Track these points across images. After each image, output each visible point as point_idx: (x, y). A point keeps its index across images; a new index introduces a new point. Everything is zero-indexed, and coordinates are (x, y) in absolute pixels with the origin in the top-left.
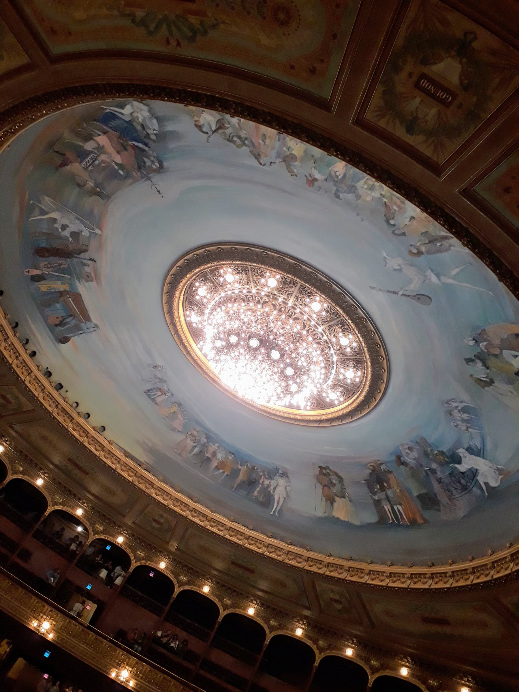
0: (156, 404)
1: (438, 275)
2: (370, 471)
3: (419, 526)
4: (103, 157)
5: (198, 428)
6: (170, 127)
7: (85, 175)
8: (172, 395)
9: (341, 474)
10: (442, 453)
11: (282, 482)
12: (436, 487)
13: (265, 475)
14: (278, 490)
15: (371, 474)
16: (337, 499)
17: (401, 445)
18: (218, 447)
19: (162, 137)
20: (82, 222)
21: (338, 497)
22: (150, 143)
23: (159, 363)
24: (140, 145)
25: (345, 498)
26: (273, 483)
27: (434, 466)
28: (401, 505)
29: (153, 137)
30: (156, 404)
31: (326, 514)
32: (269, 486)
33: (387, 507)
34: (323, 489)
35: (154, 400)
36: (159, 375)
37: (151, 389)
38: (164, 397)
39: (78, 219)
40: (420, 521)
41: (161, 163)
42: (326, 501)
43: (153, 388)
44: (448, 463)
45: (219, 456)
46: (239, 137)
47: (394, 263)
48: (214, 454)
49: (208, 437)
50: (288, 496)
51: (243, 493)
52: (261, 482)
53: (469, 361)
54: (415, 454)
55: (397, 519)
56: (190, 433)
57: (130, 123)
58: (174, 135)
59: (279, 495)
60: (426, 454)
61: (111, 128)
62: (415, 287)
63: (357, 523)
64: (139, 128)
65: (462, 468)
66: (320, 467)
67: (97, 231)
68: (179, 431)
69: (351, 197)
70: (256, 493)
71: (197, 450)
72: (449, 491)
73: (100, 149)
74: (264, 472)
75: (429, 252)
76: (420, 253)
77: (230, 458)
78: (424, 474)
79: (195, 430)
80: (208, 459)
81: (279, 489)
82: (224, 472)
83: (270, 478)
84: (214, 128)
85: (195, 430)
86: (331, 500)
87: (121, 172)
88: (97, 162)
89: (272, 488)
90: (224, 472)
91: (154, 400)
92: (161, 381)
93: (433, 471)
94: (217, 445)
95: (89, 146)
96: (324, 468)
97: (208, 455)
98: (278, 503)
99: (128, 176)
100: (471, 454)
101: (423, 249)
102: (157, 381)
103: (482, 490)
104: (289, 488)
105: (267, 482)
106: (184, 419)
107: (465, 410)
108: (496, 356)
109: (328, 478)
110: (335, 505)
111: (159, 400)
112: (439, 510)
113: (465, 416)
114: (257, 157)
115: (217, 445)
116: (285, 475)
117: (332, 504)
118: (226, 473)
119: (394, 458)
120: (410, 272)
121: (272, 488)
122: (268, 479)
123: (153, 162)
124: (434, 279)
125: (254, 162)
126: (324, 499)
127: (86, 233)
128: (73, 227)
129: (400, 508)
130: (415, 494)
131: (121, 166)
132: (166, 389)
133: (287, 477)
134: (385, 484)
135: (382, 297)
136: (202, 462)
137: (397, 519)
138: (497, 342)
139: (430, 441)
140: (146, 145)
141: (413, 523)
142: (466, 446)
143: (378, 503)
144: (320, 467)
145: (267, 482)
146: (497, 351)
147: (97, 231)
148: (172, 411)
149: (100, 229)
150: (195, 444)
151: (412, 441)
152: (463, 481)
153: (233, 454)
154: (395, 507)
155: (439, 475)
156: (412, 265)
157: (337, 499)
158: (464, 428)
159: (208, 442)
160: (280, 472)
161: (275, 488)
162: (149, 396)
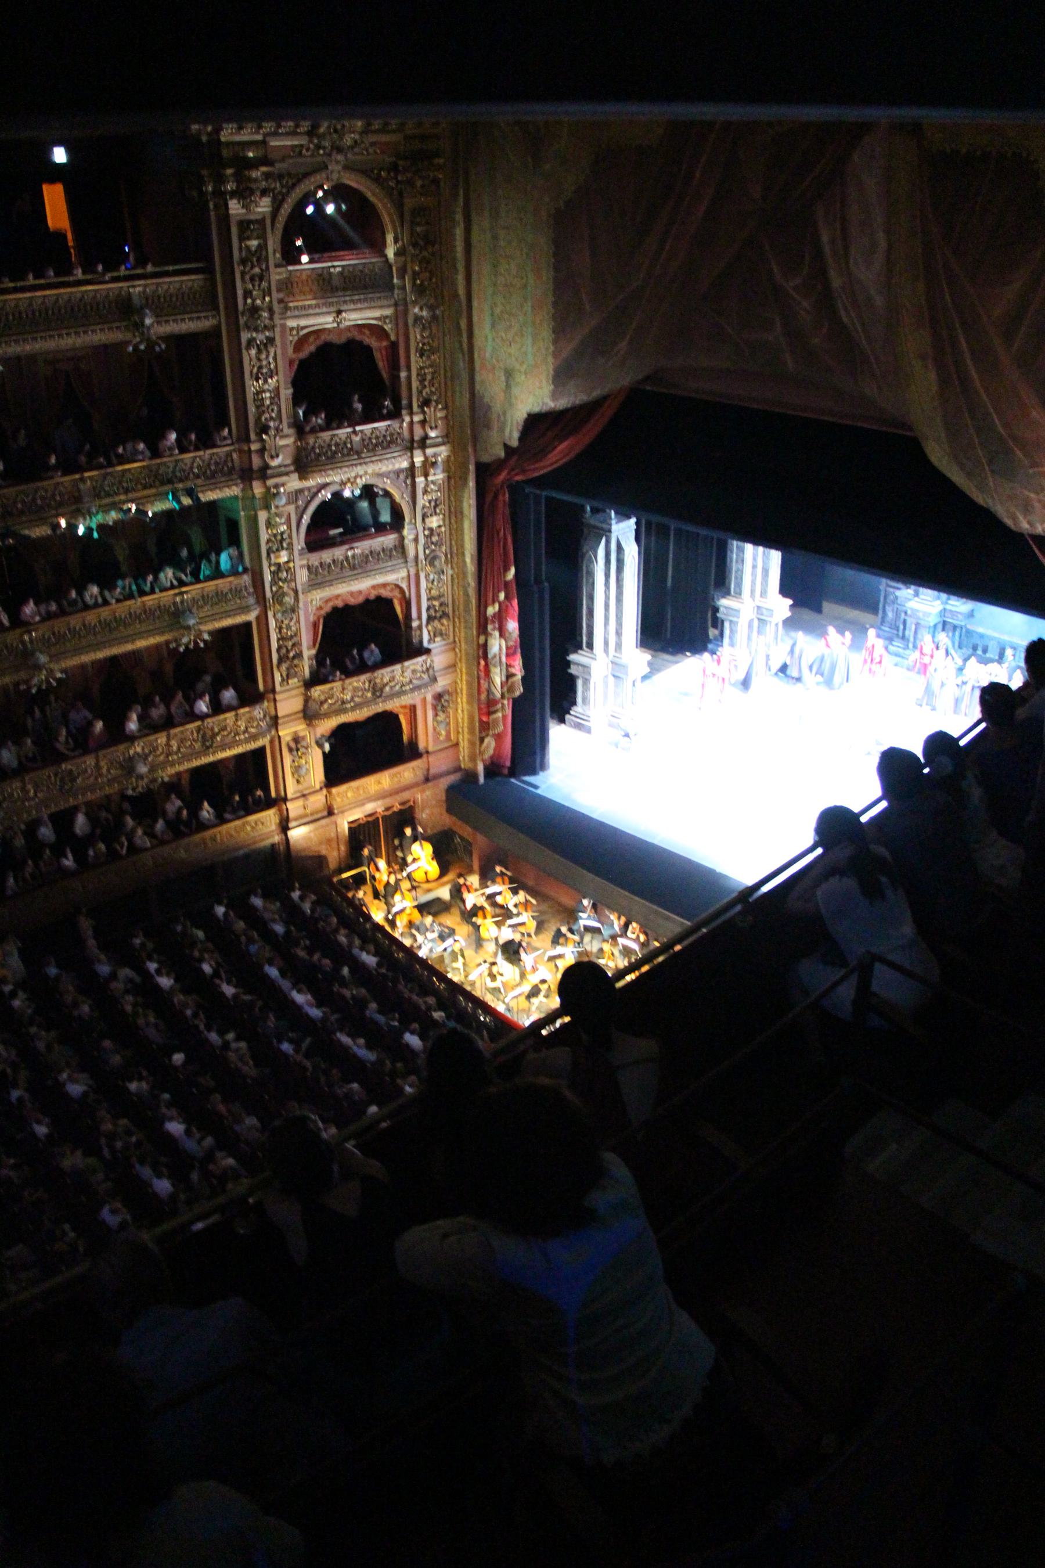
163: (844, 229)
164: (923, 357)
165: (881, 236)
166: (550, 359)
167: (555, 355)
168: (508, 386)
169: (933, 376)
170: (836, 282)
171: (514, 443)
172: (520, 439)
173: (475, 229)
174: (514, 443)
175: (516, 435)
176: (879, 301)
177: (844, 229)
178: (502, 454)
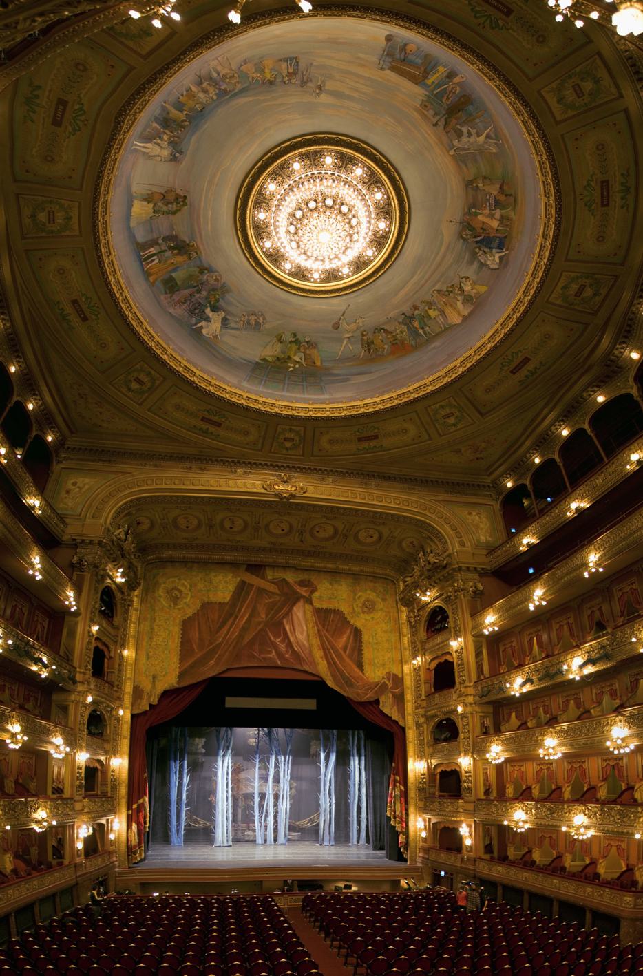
0: (280, 60)
1: (349, 338)
2: (187, 242)
3: (147, 279)
4: (487, 211)
5: (239, 87)
6: (475, 265)
7: (487, 188)
8: (285, 82)
9: (179, 214)
10: (218, 301)
11: (166, 153)
12: (187, 292)
13: (174, 137)
14: (158, 149)
15: (185, 242)
16: (151, 205)
17: (220, 275)
18: (212, 98)
19: (474, 255)
20: (464, 149)
21: (154, 206)
22: (475, 245)
23: (324, 98)
24: (478, 239)
25: (154, 212)
26: (165, 144)
27: (204, 293)
28: (160, 262)
29: (477, 250)
30: (280, 60)
31: (134, 194)
32: (161, 139)
33: (153, 250)
34: (161, 193)
35: (285, 60)
36: (310, 84)
37: (298, 65)
38: (285, 73)
39: (468, 149)
40: (151, 279)
41: (464, 239)
42: (148, 194)
43: (299, 67)
44: (210, 302)
45: (202, 95)
46: (451, 292)
47: (360, 321)
48: (205, 91)
49: (225, 92)
50: (150, 156)
51: (158, 112)
52: (166, 131)
53: (295, 335)
54: (212, 281)
55: (145, 260)
56: (236, 75)
57: (491, 249)
58: (470, 263)
59: (151, 148)
60: (214, 290)
61: (497, 237)
62: (344, 325)
63: (133, 224)
64: (486, 250)
65: (208, 311)
66: (185, 197)
67: (452, 153)
68: (241, 65)
69: (401, 320)
70: (155, 125)
71: (215, 75)
72: (186, 301)
73: (492, 216)
74: (177, 137)
75: (362, 339)
76: (363, 335)
77: (197, 106)
78: (195, 284)
79: (238, 82)
80: (201, 83)
81: (159, 150)
82: (182, 95)
83: (170, 143)
84: (462, 285)
85: (238, 82)
86: (148, 199)
87: (474, 210)
88: (488, 204)
89: (159, 141)
90: (182, 95)
91: (285, 60)
92: (303, 84)
93: (199, 291)
94: (215, 97)
95: (498, 213)
96: (184, 201)
97: (205, 85)
98: (143, 147)
99: (469, 213)
100: (222, 319)
101: (365, 338)
102: (305, 78)
103: (196, 324)
104: (159, 159)
105: (165, 137)
106: (253, 78)
107: (257, 324)
108: (299, 349)
109: (172, 201)
110: (145, 203)
111: (284, 65)
112: (166, 293)
113: (253, 322)
114: (439, 292)
115: (215, 97)
116: (173, 159)
117: (145, 200)
118: (181, 97)
119: (206, 265)
120: (353, 326)
121: (159, 141)
122: (169, 139)
123: (467, 235)
124: (347, 335)
125: (436, 288)
126: (150, 192)
127: (455, 142)
128: (465, 139)
129: (157, 261)
130: (174, 275)
131: (476, 214)
132: (293, 81)
133: (171, 160)
134: (176, 251)
135: (343, 308)
136: (200, 77)
137: (145, 260)
138: (308, 352)
139: (228, 296)
140: (477, 242)
141: (147, 274)
142: (228, 317)
143: (154, 242)
144: (185, 197)
145: (165, 137)
146: (302, 350)
147: (452, 153)
148: (266, 70)
149: (452, 156)
150: (221, 75)
151: (224, 283)
152: (197, 311)
153: (201, 111)
154: (155, 257)
155: (197, 295)
156: (357, 329)
157: (151, 205)
158: (242, 319)
159: (220, 89)
160: (177, 155)
161: (158, 145)
162: (292, 59)
163: (293, 626)
164: (322, 658)
165: (305, 627)
166: (178, 670)
167: (180, 668)
168: (154, 681)
169: (325, 662)
170: (292, 639)
171: (156, 702)
172: (159, 701)
173: (142, 626)
174: (156, 702)
175: (157, 700)
176: (305, 643)
177: (293, 626)
178: (148, 709)
